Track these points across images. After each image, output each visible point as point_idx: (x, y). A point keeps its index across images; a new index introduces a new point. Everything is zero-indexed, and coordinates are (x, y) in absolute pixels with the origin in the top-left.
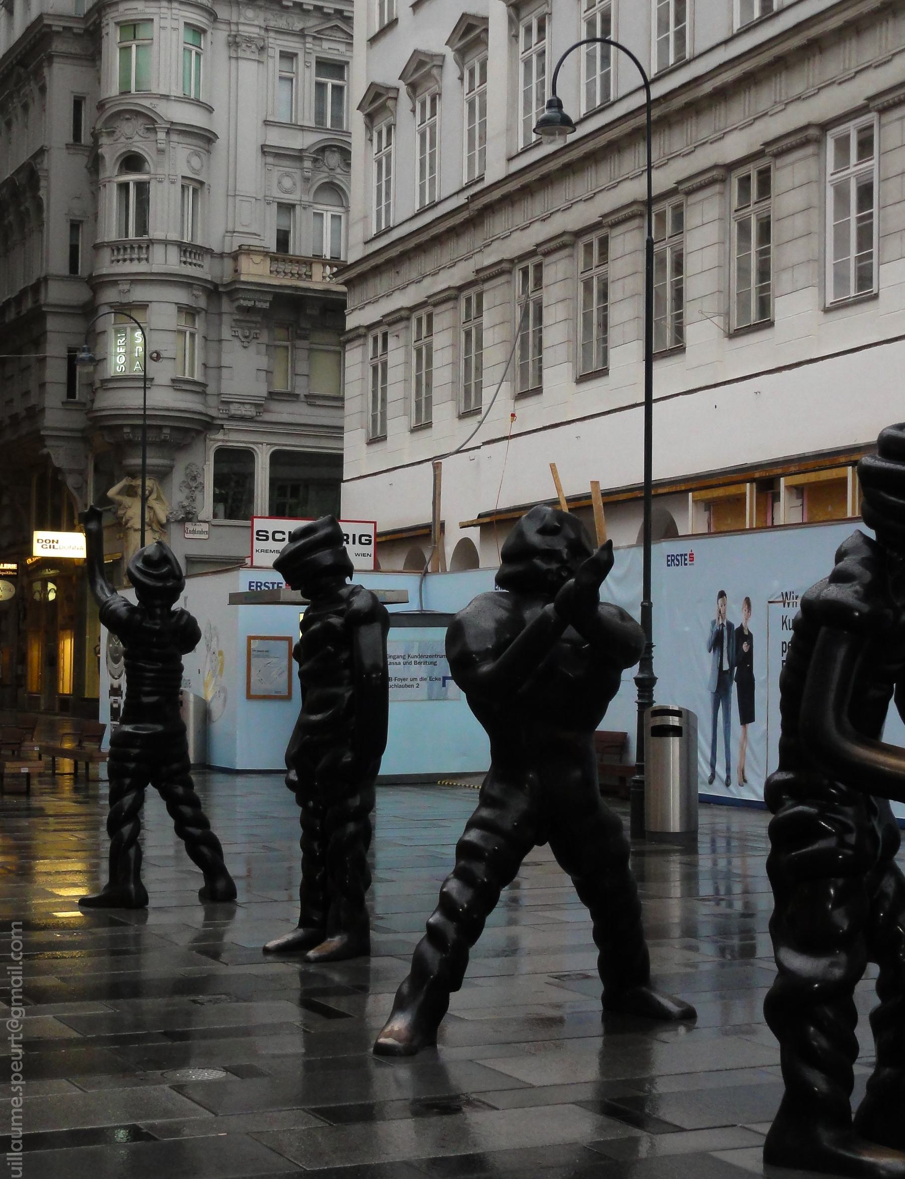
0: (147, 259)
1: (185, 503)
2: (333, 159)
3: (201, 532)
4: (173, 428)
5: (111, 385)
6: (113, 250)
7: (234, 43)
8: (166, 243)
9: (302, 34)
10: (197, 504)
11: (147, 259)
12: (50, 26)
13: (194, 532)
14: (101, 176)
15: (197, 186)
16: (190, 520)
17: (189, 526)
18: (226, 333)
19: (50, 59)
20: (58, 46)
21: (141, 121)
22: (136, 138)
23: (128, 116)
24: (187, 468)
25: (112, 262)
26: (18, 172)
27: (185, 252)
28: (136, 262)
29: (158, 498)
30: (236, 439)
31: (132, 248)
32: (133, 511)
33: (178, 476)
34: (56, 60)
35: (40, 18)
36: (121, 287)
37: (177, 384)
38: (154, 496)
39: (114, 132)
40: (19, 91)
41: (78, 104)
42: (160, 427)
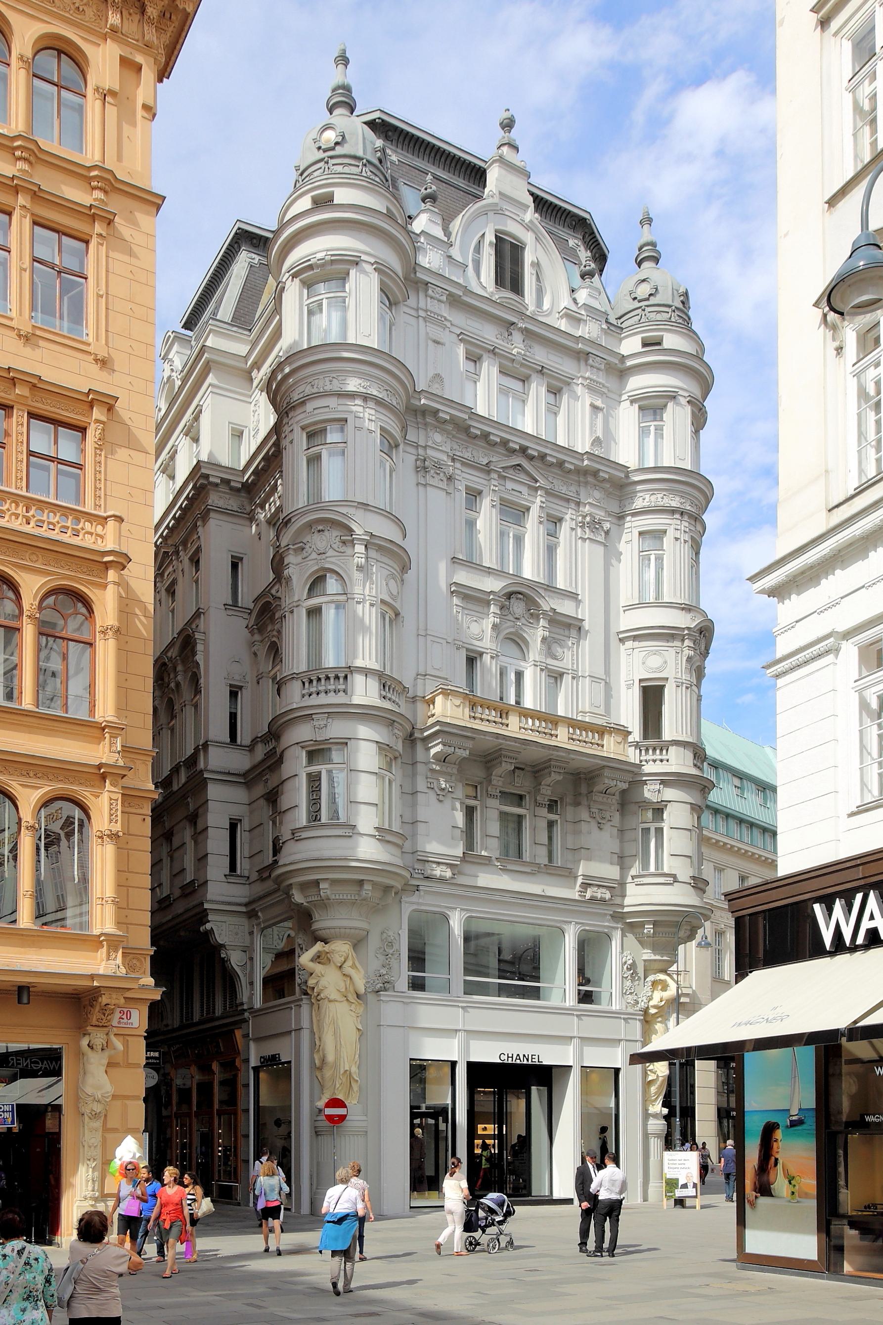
1: (383, 971)
7: (422, 467)
21: (335, 533)
22: (331, 553)
23: (320, 528)
29: (354, 966)
33: (374, 942)
38: (349, 963)
39: (303, 549)
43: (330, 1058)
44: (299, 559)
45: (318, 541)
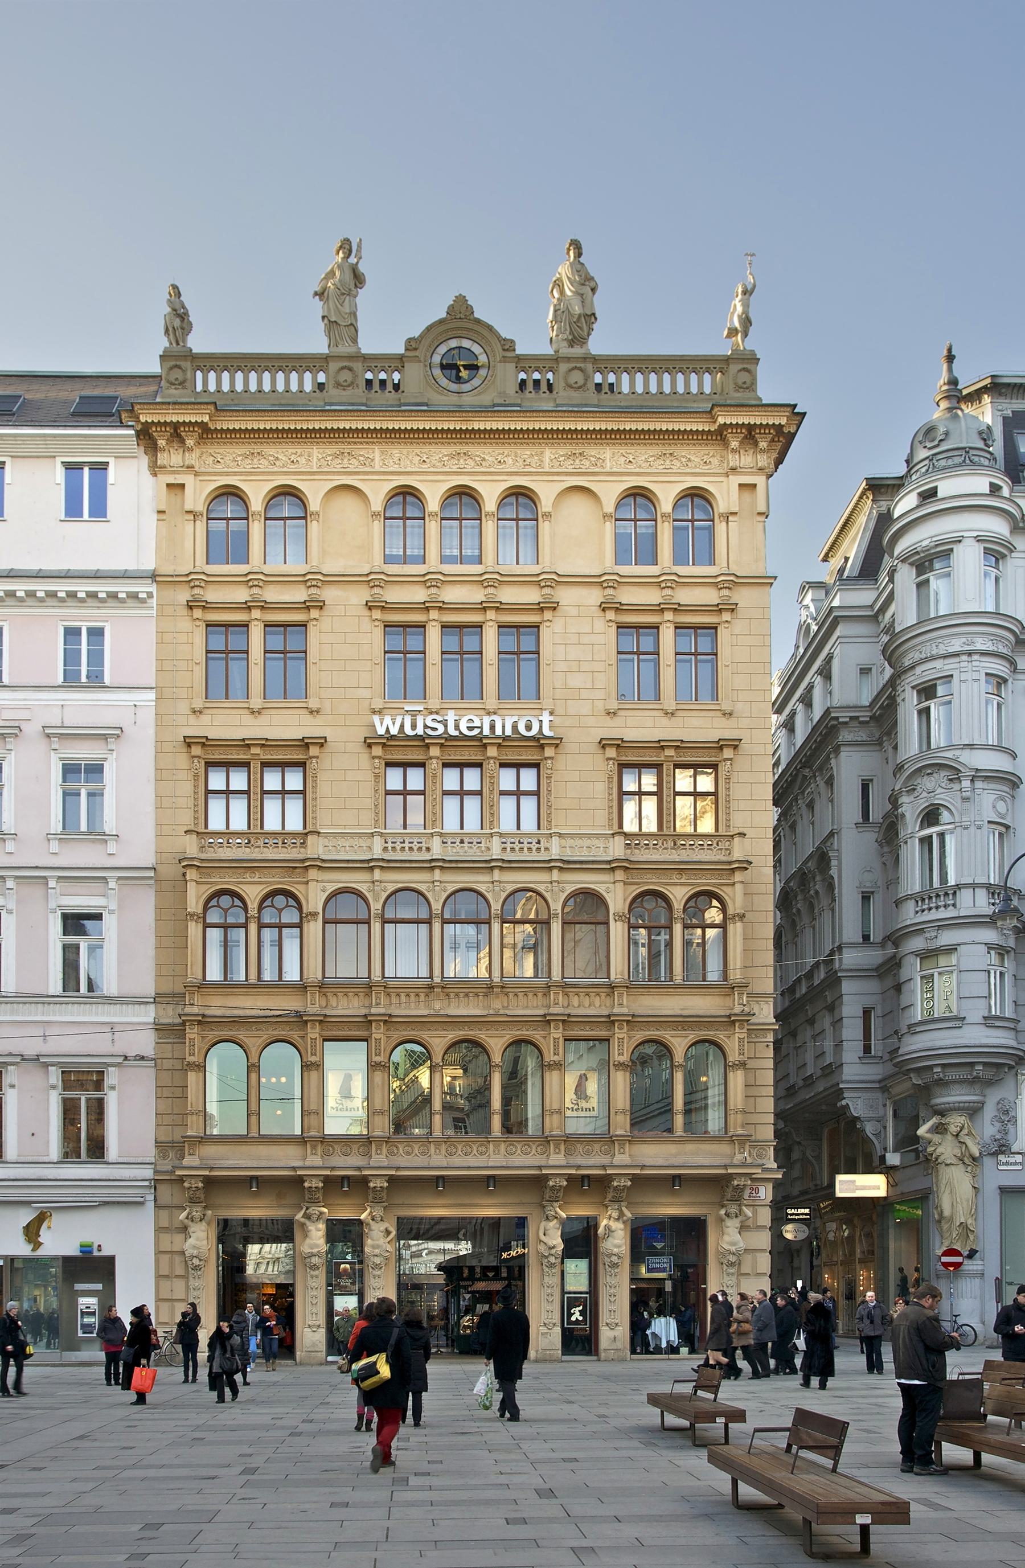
1: (998, 1137)
3: (1016, 1164)
4: (985, 1064)
10: (1011, 1137)
12: (837, 718)
13: (1007, 1164)
14: (902, 834)
15: (1003, 830)
16: (1003, 1153)
17: (1001, 1157)
19: (837, 750)
20: (845, 735)
24: (998, 1103)
25: (917, 912)
26: (805, 863)
27: (993, 894)
31: (938, 896)
32: (946, 1149)
33: (990, 1111)
34: (842, 748)
35: (827, 712)
36: (928, 935)
37: (989, 1021)
40: (803, 792)
41: (865, 788)
42: (972, 1064)
43: (947, 1213)
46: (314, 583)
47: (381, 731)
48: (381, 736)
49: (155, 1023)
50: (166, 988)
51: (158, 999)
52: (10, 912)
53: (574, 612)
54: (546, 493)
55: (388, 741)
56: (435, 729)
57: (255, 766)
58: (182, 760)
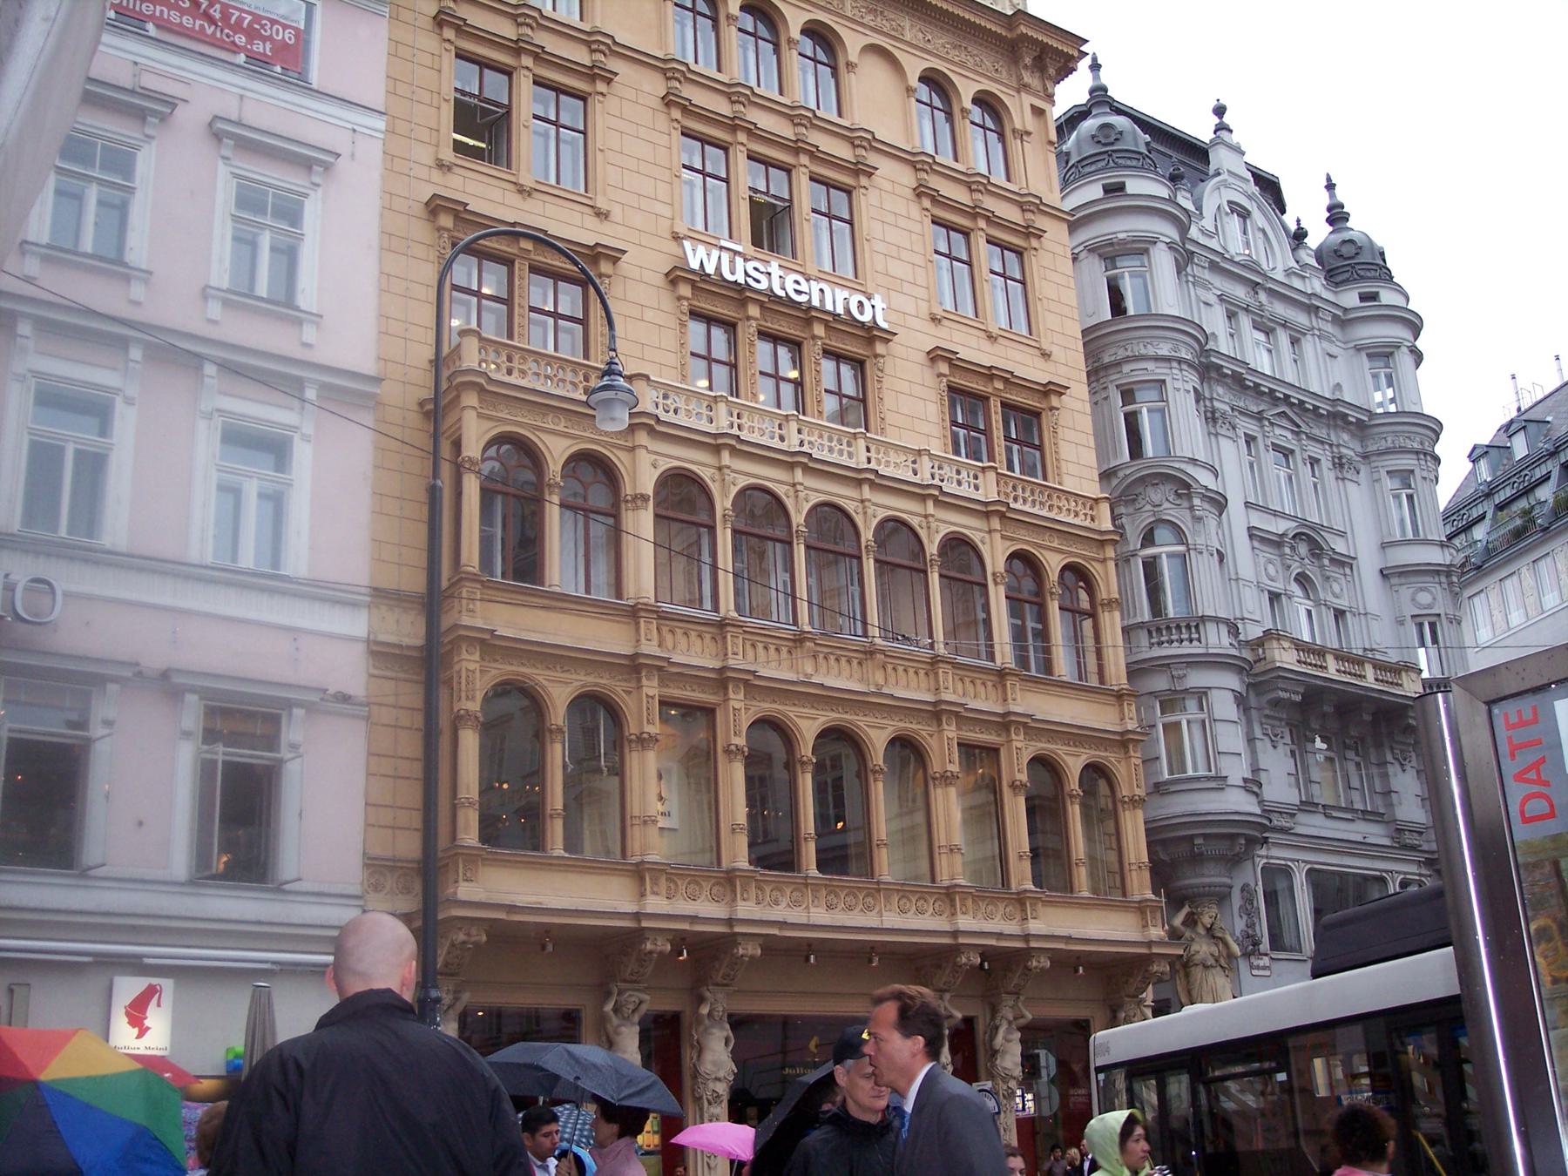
0: (1199, 640)
2: (1303, 549)
3: (1264, 968)
5: (1173, 788)
6: (1150, 632)
8: (1217, 620)
9: (1259, 417)
11: (1199, 640)
13: (1258, 968)
18: (1258, 733)
28: (1175, 644)
30: (1278, 854)
33: (1236, 899)
44: (1131, 510)
45: (1155, 495)
46: (602, 47)
47: (695, 265)
48: (693, 272)
49: (368, 641)
50: (389, 581)
51: (381, 595)
52: (129, 402)
53: (887, 186)
54: (853, 42)
55: (701, 282)
56: (758, 281)
57: (521, 268)
58: (421, 230)
